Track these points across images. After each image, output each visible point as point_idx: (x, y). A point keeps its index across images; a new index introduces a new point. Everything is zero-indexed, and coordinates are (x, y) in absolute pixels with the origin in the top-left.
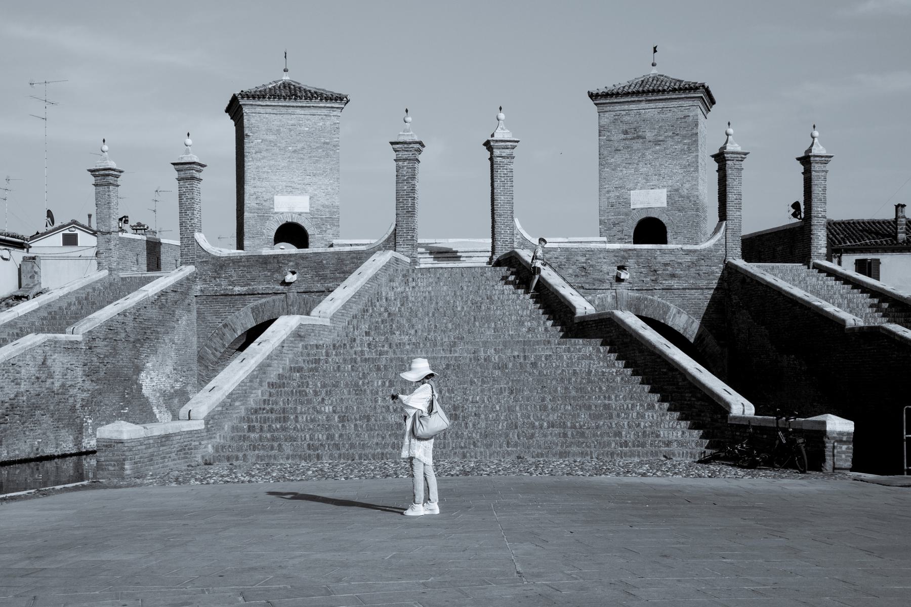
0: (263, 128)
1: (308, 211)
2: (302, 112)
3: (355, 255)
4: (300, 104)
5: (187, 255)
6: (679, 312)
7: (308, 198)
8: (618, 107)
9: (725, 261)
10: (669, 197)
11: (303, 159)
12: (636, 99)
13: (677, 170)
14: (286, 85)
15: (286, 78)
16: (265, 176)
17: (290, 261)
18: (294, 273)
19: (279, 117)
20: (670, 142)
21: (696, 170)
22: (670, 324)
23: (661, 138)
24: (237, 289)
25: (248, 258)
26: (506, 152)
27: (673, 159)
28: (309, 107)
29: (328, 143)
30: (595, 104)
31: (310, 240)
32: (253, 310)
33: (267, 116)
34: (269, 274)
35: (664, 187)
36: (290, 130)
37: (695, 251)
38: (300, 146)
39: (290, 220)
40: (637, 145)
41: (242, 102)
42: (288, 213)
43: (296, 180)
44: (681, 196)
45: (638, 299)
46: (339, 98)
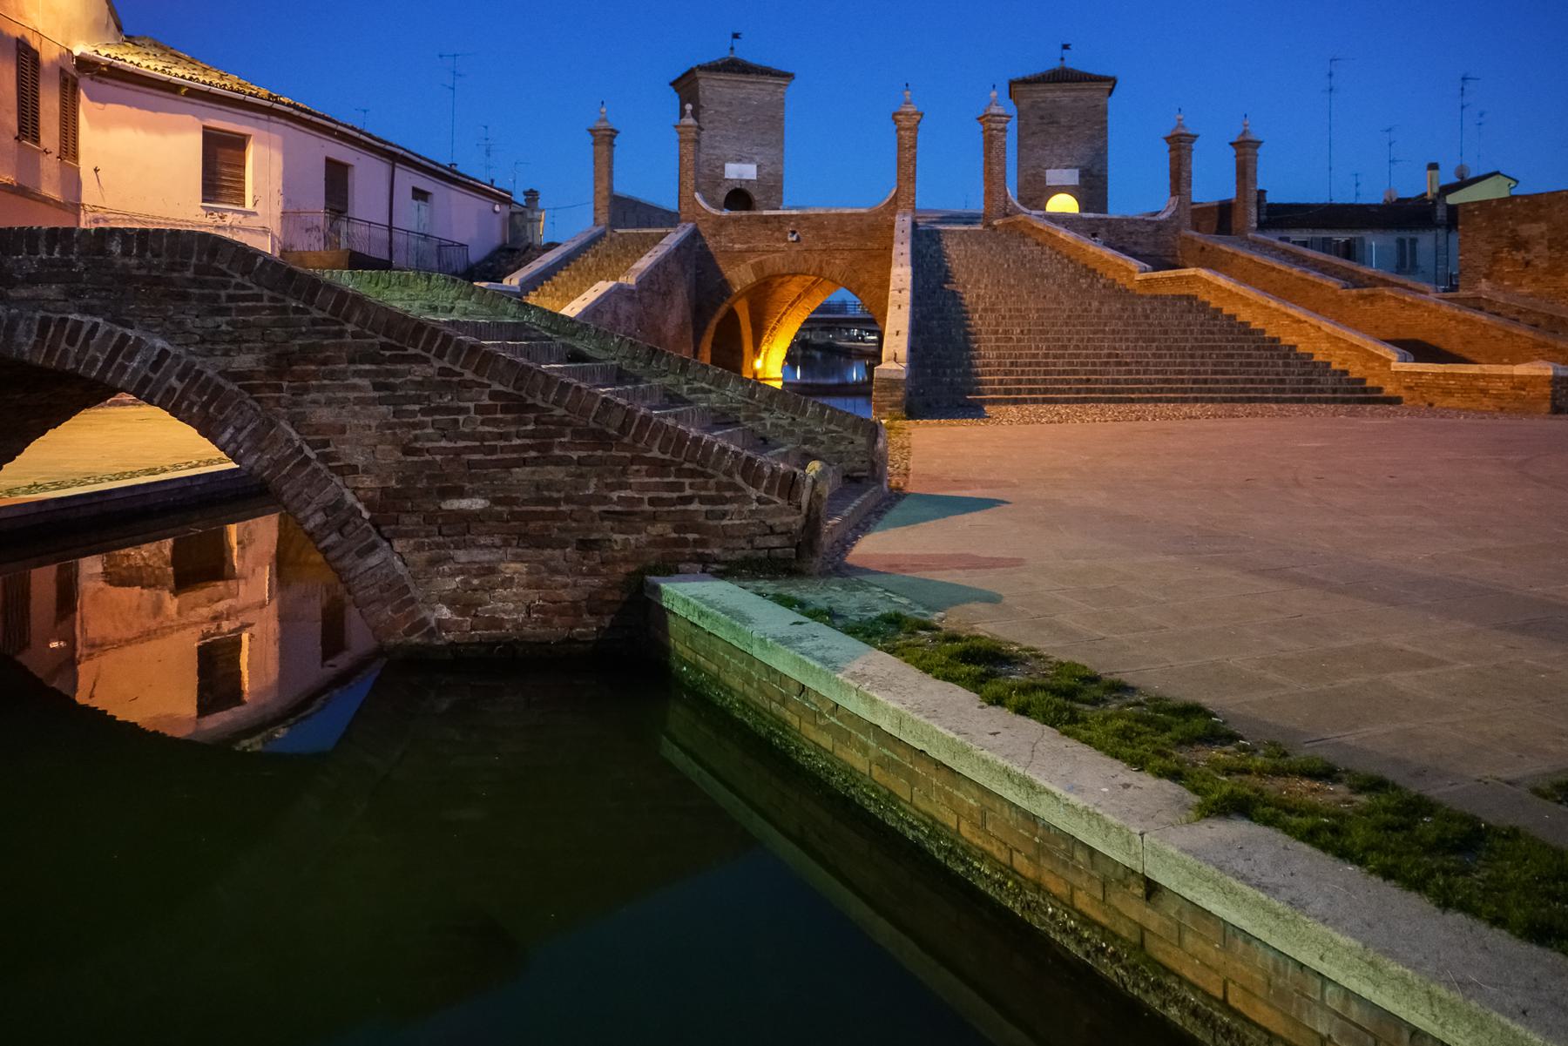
7: (755, 166)
8: (1035, 95)
23: (1075, 124)
29: (774, 117)
31: (757, 204)
35: (1076, 167)
36: (741, 104)
38: (749, 119)
39: (738, 187)
40: (1053, 130)
41: (699, 74)
44: (1092, 175)
46: (788, 76)
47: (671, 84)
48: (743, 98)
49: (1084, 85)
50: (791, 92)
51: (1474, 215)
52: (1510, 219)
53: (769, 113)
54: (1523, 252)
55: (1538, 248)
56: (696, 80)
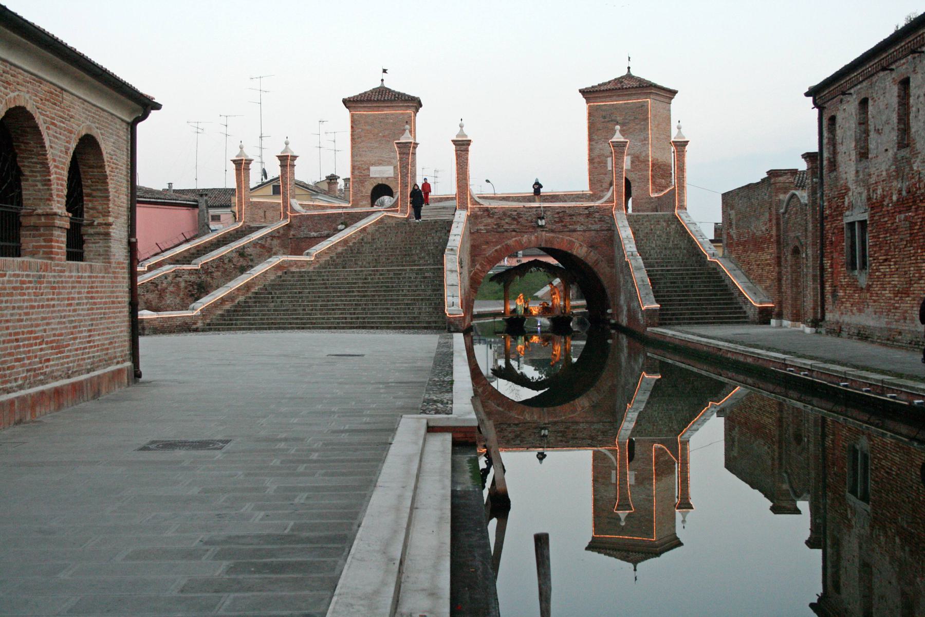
0: (363, 122)
4: (387, 105)
6: (581, 246)
7: (392, 168)
10: (632, 162)
11: (389, 141)
12: (610, 94)
16: (364, 153)
22: (575, 253)
23: (627, 121)
24: (313, 234)
26: (463, 148)
28: (392, 106)
30: (585, 98)
36: (381, 122)
38: (387, 133)
39: (380, 183)
42: (378, 178)
43: (384, 156)
45: (553, 237)
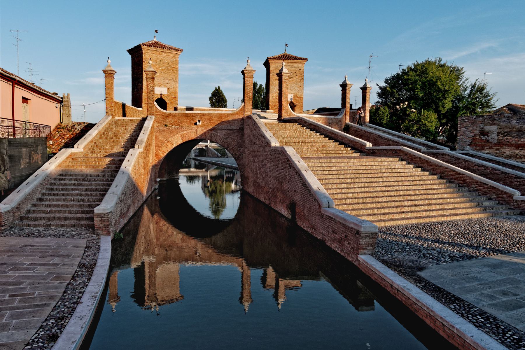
1: (167, 94)
2: (165, 54)
3: (226, 115)
4: (165, 51)
5: (150, 111)
7: (166, 89)
8: (277, 64)
9: (345, 122)
13: (296, 88)
14: (156, 43)
15: (155, 40)
17: (198, 116)
18: (199, 121)
19: (156, 55)
20: (294, 78)
21: (303, 89)
25: (179, 114)
27: (295, 84)
29: (174, 68)
32: (181, 135)
33: (152, 54)
34: (188, 121)
36: (160, 61)
37: (337, 119)
38: (164, 68)
41: (143, 47)
47: (127, 51)
48: (161, 59)
49: (296, 61)
50: (180, 57)
51: (465, 121)
52: (482, 123)
53: (173, 66)
54: (486, 136)
55: (493, 135)
56: (141, 50)
